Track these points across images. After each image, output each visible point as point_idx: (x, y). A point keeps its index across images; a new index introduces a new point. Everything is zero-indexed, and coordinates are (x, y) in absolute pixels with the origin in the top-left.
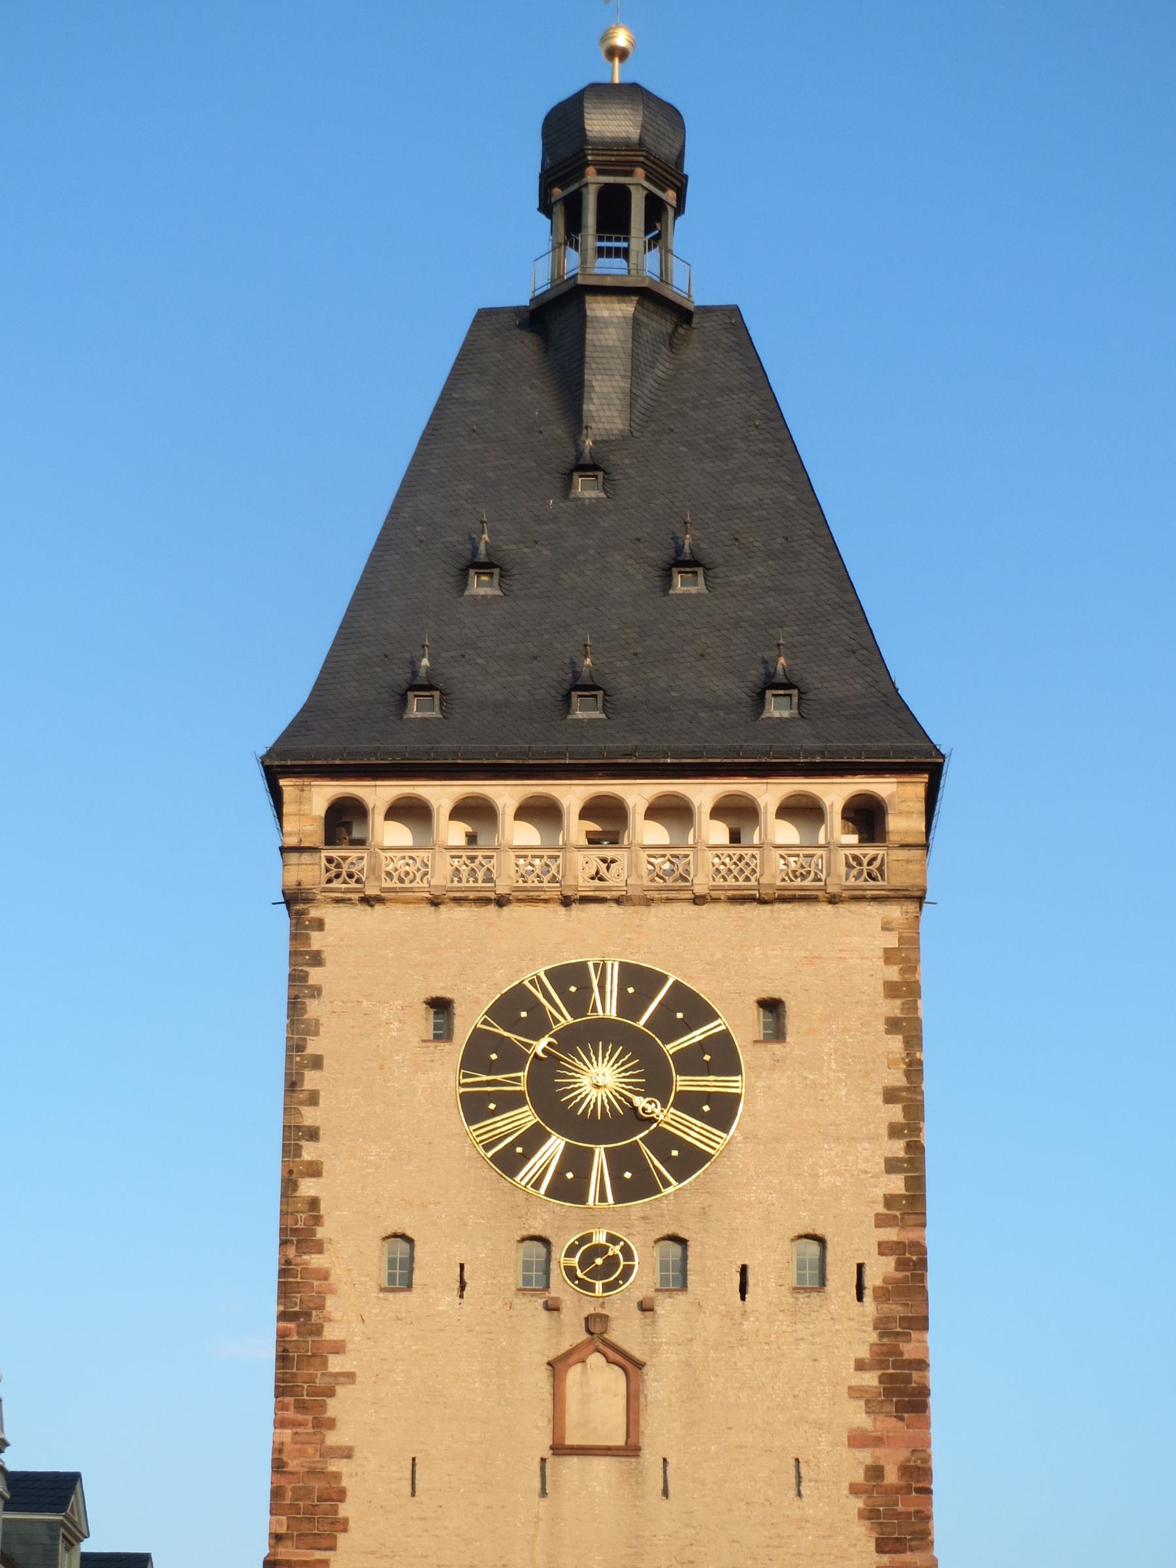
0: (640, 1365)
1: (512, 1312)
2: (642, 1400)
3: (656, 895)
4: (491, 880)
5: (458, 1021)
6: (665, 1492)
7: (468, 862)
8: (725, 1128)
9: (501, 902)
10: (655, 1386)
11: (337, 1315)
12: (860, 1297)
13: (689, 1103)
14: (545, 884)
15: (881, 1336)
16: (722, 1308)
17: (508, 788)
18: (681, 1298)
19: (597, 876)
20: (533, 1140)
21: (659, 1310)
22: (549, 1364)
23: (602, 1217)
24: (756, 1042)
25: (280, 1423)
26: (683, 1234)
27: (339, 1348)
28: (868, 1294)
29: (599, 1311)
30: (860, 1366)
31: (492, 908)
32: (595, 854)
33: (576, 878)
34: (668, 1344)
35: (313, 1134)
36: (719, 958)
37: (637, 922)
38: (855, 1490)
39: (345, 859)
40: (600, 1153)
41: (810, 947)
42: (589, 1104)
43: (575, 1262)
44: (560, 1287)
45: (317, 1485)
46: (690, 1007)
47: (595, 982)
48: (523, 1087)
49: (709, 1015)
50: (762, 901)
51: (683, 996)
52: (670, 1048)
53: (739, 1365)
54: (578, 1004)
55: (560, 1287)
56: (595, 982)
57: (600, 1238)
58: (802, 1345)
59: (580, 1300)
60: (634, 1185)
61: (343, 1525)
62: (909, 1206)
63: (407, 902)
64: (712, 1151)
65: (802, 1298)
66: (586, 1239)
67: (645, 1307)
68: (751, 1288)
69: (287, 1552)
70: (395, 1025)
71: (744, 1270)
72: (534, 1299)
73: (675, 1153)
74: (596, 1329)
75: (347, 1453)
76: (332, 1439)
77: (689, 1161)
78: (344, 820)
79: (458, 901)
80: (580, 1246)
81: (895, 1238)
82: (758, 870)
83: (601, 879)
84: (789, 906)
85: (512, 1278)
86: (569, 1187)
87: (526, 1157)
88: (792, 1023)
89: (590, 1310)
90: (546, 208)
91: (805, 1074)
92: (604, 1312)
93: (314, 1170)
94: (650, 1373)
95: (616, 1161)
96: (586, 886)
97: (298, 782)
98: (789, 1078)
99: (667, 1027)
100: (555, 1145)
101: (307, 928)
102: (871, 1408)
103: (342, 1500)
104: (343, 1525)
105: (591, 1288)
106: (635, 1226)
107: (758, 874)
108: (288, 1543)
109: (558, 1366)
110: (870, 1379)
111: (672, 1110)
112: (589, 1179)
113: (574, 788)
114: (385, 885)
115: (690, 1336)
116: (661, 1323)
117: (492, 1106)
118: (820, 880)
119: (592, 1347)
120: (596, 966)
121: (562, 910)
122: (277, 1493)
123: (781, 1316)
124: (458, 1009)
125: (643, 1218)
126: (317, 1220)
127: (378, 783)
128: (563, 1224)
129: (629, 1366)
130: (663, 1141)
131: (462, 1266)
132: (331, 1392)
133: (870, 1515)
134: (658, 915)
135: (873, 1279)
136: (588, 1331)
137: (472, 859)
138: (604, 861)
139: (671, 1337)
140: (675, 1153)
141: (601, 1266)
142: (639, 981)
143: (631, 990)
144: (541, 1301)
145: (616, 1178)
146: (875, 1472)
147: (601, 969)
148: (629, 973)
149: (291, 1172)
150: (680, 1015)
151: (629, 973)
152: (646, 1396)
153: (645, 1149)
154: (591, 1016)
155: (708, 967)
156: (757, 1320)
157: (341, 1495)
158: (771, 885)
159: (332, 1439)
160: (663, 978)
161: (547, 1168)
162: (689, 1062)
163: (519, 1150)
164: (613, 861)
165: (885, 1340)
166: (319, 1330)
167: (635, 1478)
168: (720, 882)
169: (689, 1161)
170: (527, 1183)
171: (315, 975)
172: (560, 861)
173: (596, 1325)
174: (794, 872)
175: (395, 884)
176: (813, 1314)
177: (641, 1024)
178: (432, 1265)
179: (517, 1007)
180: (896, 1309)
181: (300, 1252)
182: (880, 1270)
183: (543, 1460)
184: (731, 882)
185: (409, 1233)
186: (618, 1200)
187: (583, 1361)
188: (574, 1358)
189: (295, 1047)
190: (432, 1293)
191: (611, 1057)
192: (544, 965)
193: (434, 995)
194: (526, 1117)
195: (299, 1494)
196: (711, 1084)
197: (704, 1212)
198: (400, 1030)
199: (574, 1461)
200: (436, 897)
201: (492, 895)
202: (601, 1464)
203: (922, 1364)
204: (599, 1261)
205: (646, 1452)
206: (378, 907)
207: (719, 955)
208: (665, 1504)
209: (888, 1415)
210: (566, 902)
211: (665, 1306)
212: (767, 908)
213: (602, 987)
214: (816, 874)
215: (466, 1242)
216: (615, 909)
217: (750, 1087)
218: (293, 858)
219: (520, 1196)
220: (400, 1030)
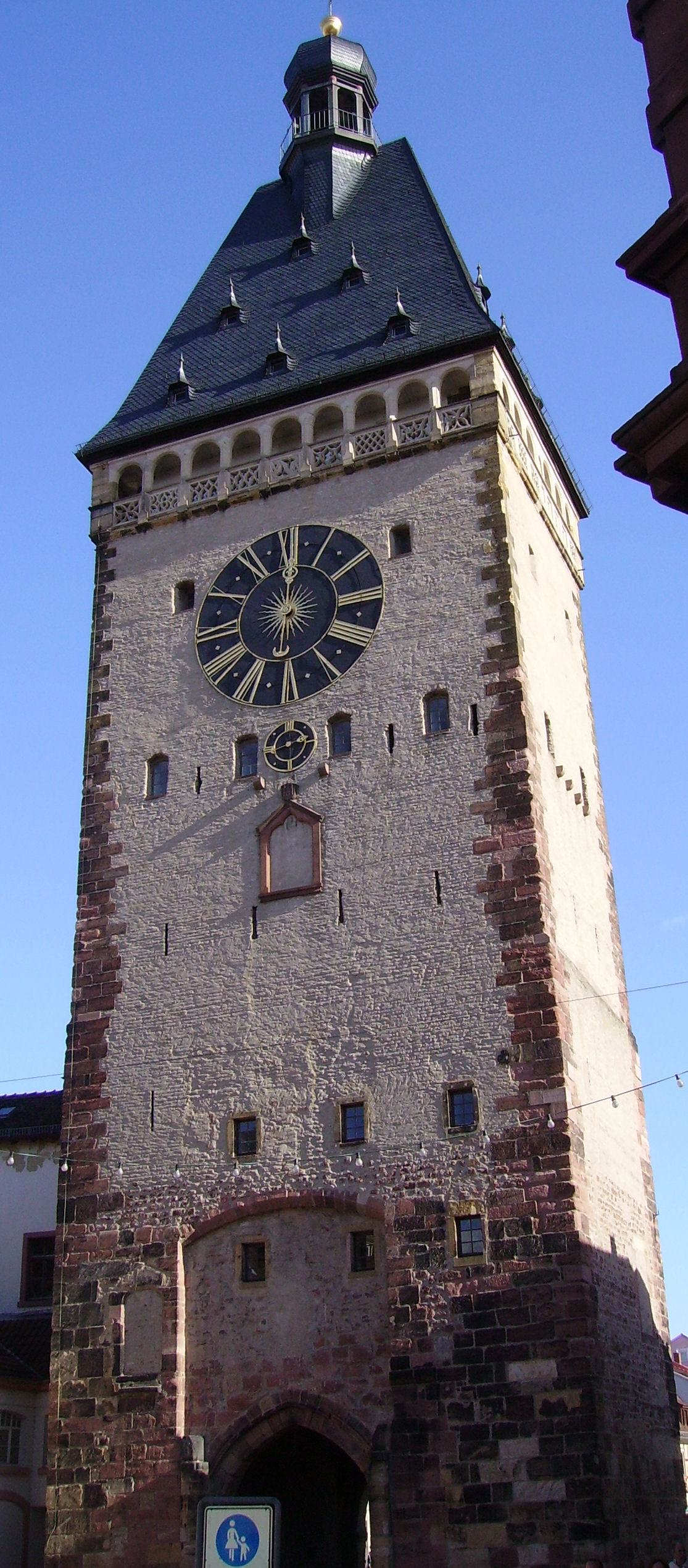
8: (374, 627)
11: (117, 824)
12: (476, 733)
15: (492, 758)
19: (283, 472)
25: (81, 915)
27: (118, 849)
28: (481, 727)
30: (478, 787)
35: (105, 696)
38: (480, 890)
39: (127, 506)
45: (103, 959)
47: (283, 545)
52: (335, 577)
54: (274, 563)
56: (283, 545)
57: (290, 727)
61: (118, 987)
62: (507, 652)
63: (165, 523)
68: (396, 743)
69: (83, 1017)
75: (122, 930)
76: (114, 920)
77: (351, 653)
78: (129, 483)
79: (197, 513)
81: (498, 680)
87: (240, 678)
93: (105, 722)
95: (299, 666)
97: (99, 464)
101: (106, 557)
102: (490, 816)
103: (118, 968)
104: (118, 987)
105: (284, 766)
106: (313, 713)
108: (83, 1008)
110: (487, 795)
120: (284, 533)
121: (262, 503)
122: (76, 970)
126: (106, 757)
128: (261, 722)
132: (112, 884)
133: (493, 908)
135: (484, 714)
142: (312, 535)
146: (495, 870)
147: (287, 535)
149: (91, 726)
153: (318, 653)
157: (117, 964)
159: (114, 920)
160: (329, 529)
163: (236, 675)
165: (495, 762)
166: (105, 838)
169: (351, 653)
171: (110, 588)
175: (157, 512)
180: (502, 736)
181: (95, 783)
182: (488, 706)
183: (254, 908)
189: (97, 638)
194: (239, 650)
195: (92, 968)
203: (524, 776)
204: (288, 744)
209: (501, 822)
210: (265, 494)
218: (97, 513)
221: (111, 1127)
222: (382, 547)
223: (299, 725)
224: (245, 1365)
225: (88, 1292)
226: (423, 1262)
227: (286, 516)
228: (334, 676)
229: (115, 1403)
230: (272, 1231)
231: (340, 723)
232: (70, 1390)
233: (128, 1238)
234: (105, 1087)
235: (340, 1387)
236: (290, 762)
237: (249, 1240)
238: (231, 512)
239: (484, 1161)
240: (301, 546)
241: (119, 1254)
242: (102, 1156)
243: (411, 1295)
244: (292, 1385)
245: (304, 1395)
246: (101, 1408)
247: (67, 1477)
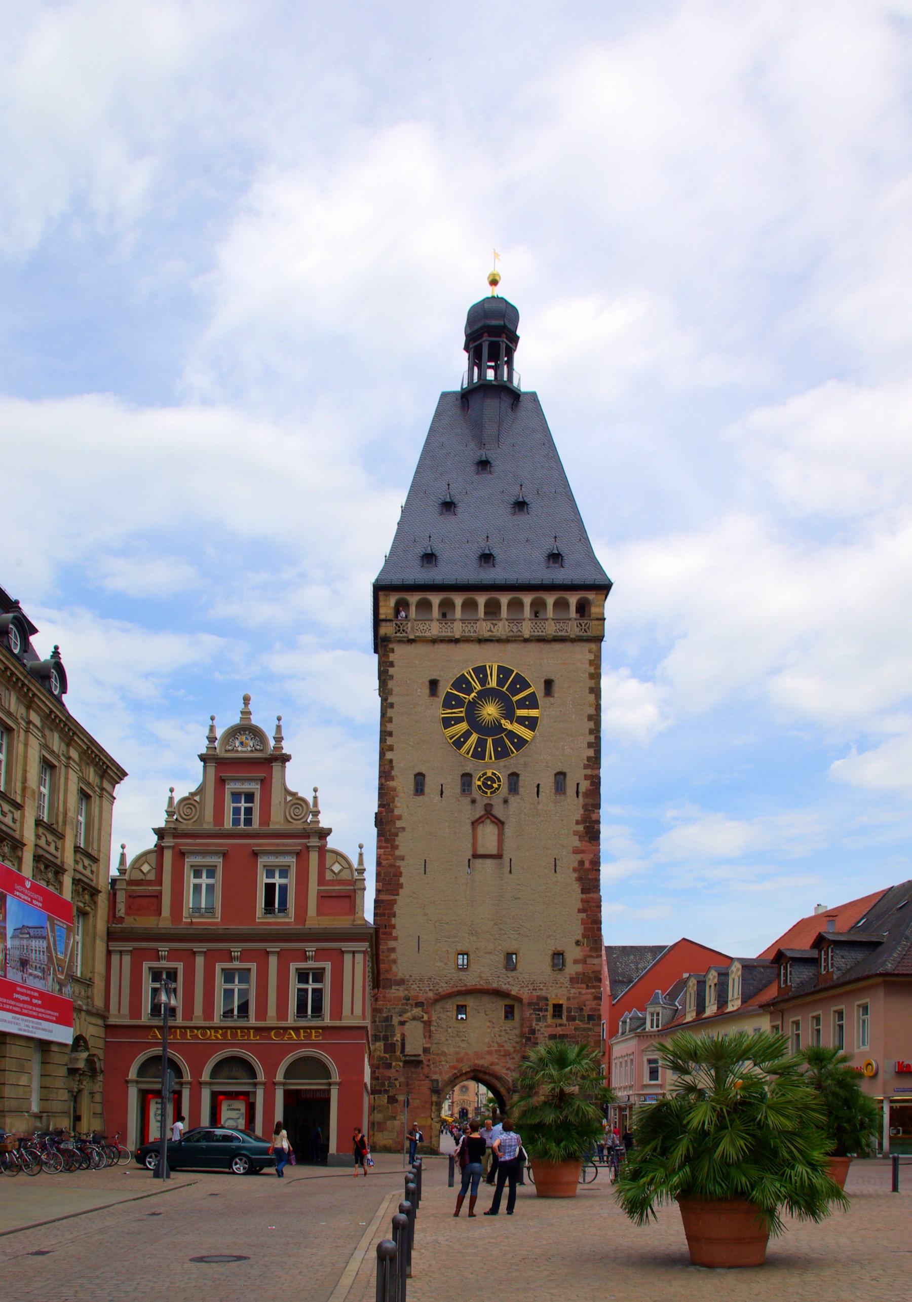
0: (503, 823)
6: (510, 872)
9: (457, 641)
10: (509, 831)
13: (521, 721)
18: (517, 797)
20: (467, 735)
32: (489, 623)
36: (531, 663)
40: (490, 741)
44: (476, 793)
46: (521, 683)
52: (515, 699)
54: (483, 682)
55: (476, 793)
57: (489, 774)
66: (485, 774)
71: (538, 785)
85: (458, 790)
86: (479, 754)
87: (464, 742)
88: (556, 688)
89: (486, 801)
90: (467, 348)
94: (506, 826)
96: (487, 635)
100: (474, 737)
102: (581, 838)
121: (477, 645)
130: (511, 735)
134: (511, 647)
139: (515, 811)
141: (489, 783)
142: (504, 672)
144: (469, 799)
151: (500, 668)
154: (488, 686)
167: (501, 866)
169: (521, 743)
173: (488, 808)
177: (504, 689)
179: (461, 683)
194: (463, 726)
197: (526, 764)
199: (480, 861)
202: (489, 861)
205: (504, 856)
208: (510, 876)
211: (513, 800)
217: (541, 714)
219: (462, 758)
221: (398, 950)
222: (536, 688)
223: (493, 774)
224: (457, 1053)
225: (388, 1019)
226: (539, 1020)
227: (493, 659)
228: (513, 752)
229: (401, 1064)
230: (470, 1002)
231: (514, 777)
232: (380, 1058)
233: (407, 999)
234: (394, 931)
235: (497, 1064)
236: (489, 792)
237: (459, 1003)
238: (461, 646)
239: (568, 984)
240: (498, 676)
241: (403, 1005)
242: (395, 962)
243: (533, 1032)
244: (477, 1062)
245: (482, 1066)
246: (395, 1067)
247: (379, 1092)
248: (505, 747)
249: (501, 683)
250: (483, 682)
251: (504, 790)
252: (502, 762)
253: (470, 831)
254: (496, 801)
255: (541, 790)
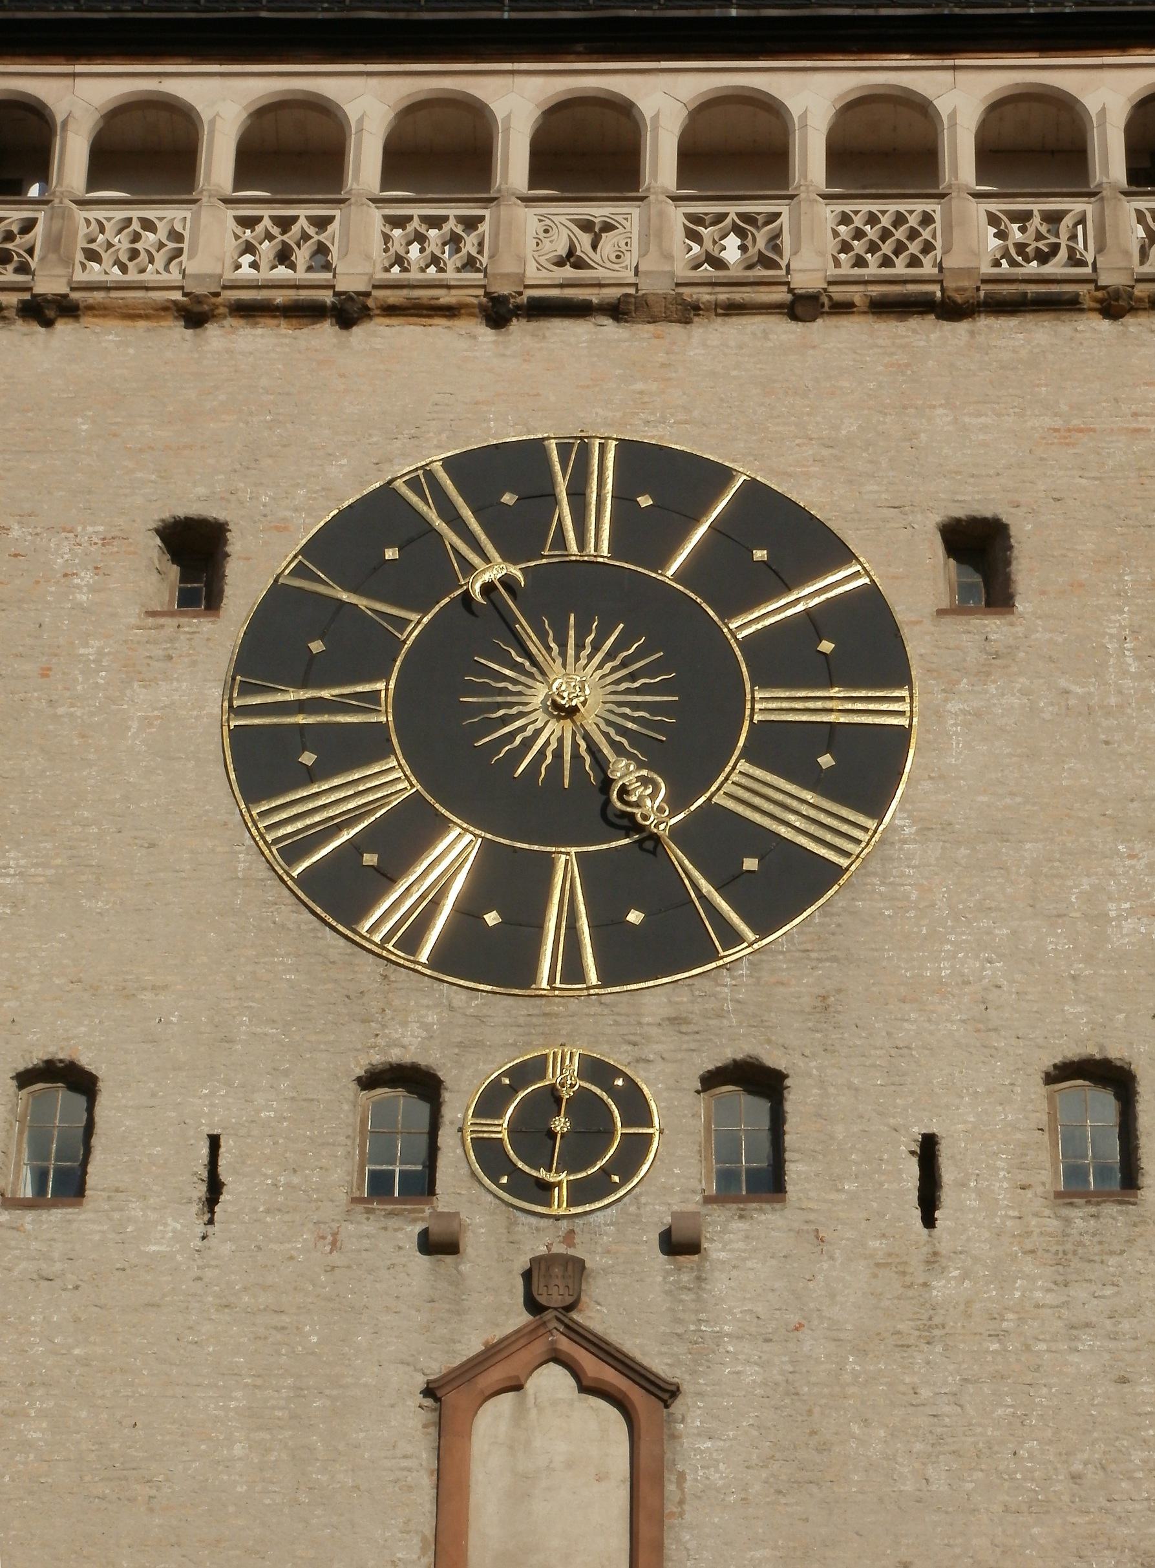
0: (666, 1393)
1: (336, 1258)
2: (671, 1487)
3: (704, 295)
4: (327, 267)
5: (234, 570)
7: (275, 231)
8: (876, 810)
9: (348, 312)
10: (708, 1448)
14: (451, 275)
16: (875, 1244)
17: (373, 82)
18: (768, 1221)
19: (571, 258)
20: (402, 837)
21: (714, 1249)
22: (430, 1391)
23: (577, 1020)
24: (941, 612)
26: (773, 1059)
29: (559, 1249)
31: (327, 330)
32: (564, 213)
33: (522, 260)
34: (737, 1337)
36: (850, 428)
37: (661, 357)
40: (566, 863)
41: (1064, 408)
42: (542, 753)
43: (500, 1129)
48: (385, 716)
49: (837, 552)
50: (951, 310)
51: (766, 511)
53: (925, 1393)
58: (1087, 1341)
59: (511, 1224)
60: (652, 940)
63: (131, 314)
64: (843, 862)
65: (1079, 1217)
67: (679, 1244)
68: (947, 1195)
70: (87, 577)
71: (928, 1151)
72: (393, 1223)
73: (751, 864)
74: (553, 1295)
77: (786, 883)
79: (249, 311)
80: (514, 1089)
82: (938, 244)
83: (579, 264)
84: (1012, 322)
85: (339, 1171)
87: (387, 876)
88: (1026, 572)
91: (1063, 683)
92: (571, 1252)
94: (691, 1415)
98: (1025, 692)
99: (732, 577)
107: (938, 252)
109: (451, 1398)
111: (743, 766)
112: (541, 927)
113: (520, 80)
114: (80, 276)
115: (795, 1319)
116: (720, 1284)
117: (308, 758)
118: (1081, 263)
119: (539, 1348)
121: (486, 334)
123: (1029, 1266)
124: (236, 545)
125: (675, 1021)
127: (79, 68)
128: (471, 1037)
129: (636, 1395)
130: (720, 839)
131: (214, 1142)
136: (533, 1305)
137: (285, 224)
138: (586, 226)
140: (751, 864)
141: (570, 1134)
142: (665, 481)
143: (645, 501)
145: (607, 927)
148: (642, 462)
150: (760, 555)
152: (681, 1476)
153: (677, 855)
155: (826, 452)
156: (965, 1276)
158: (969, 272)
160: (725, 475)
161: (436, 903)
162: (786, 656)
163: (370, 859)
164: (608, 227)
168: (846, 270)
170: (387, 938)
172: (484, 227)
173: (551, 1294)
174: (1021, 248)
176: (1112, 1261)
178: (139, 1142)
179: (373, 537)
184: (873, 269)
185: (86, 1060)
186: (608, 977)
187: (517, 1387)
188: (496, 1375)
190: (135, 1209)
191: (596, 648)
192: (440, 447)
193: (182, 512)
196: (838, 705)
197: (824, 1005)
198: (93, 589)
200: (197, 299)
201: (327, 297)
204: (561, 1124)
206: (63, 327)
207: (850, 426)
210: (498, 313)
212: (963, 327)
213: (578, 495)
214: (1072, 251)
215: (228, 1083)
216: (609, 328)
220: (93, 589)
223: (596, 1070)
238: (377, 336)
240: (624, 497)
248: (671, 901)
249: (642, 536)
250: (520, 533)
251: (675, 1166)
252: (656, 996)
253: (424, 1456)
254: (616, 1242)
255: (948, 1173)
